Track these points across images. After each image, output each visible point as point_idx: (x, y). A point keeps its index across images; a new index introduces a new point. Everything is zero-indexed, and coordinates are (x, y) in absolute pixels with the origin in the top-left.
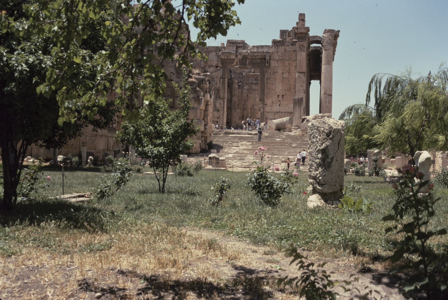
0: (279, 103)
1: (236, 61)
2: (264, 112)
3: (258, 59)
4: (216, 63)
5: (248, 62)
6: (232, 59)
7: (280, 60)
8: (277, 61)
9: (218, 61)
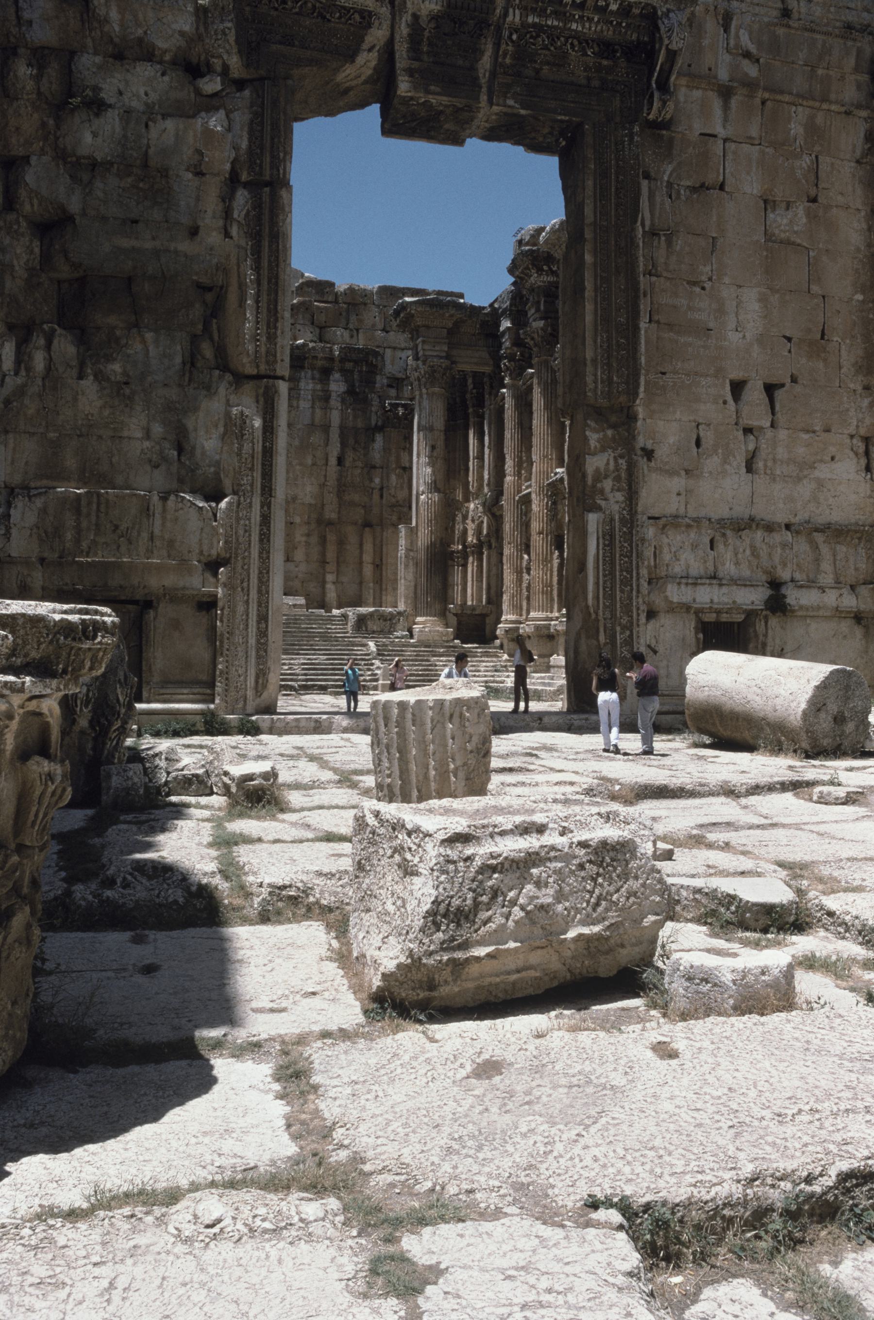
0: (742, 447)
1: (377, 35)
2: (630, 520)
3: (583, 41)
7: (751, 85)
8: (726, 93)
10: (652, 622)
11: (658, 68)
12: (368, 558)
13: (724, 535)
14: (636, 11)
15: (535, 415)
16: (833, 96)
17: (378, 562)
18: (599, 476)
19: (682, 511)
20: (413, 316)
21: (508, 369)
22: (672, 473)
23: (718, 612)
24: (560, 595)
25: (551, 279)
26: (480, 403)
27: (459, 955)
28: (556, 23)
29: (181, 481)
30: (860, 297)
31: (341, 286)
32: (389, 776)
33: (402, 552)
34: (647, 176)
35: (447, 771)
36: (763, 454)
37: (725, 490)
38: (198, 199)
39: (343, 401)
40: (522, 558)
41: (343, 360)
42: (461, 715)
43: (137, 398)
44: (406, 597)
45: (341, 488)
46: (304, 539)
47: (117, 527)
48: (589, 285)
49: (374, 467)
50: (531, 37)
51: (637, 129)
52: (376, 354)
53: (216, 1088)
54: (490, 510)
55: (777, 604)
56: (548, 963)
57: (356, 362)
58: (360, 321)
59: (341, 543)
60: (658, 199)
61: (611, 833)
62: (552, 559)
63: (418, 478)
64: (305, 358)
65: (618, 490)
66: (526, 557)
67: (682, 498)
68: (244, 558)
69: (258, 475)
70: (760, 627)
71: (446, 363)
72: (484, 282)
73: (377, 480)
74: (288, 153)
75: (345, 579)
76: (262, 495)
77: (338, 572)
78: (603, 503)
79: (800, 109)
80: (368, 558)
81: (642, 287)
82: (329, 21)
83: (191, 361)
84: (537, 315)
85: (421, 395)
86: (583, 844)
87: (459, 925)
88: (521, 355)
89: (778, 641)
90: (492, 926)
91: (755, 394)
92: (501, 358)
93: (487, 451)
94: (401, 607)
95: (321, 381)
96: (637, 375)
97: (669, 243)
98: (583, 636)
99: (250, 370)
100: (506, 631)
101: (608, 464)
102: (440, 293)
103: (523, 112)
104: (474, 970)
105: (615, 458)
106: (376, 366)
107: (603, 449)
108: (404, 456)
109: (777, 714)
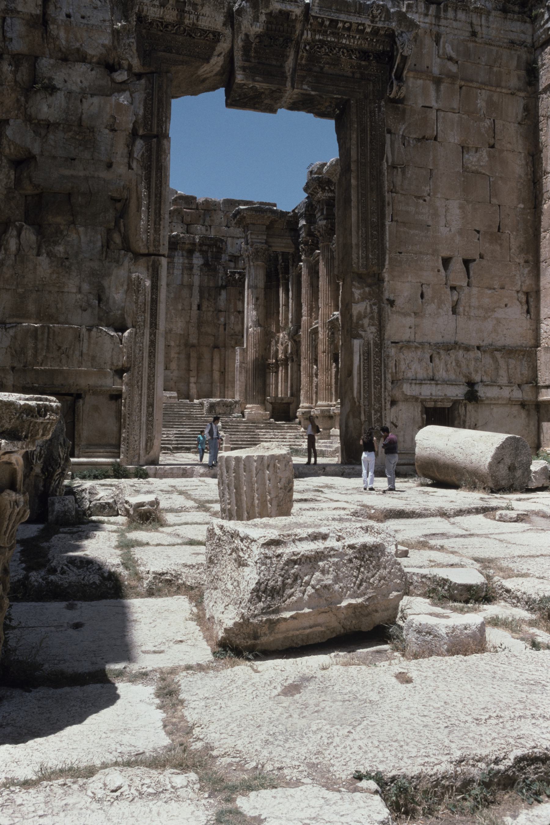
0: (449, 298)
1: (223, 46)
2: (380, 344)
3: (350, 50)
4: (106, 40)
5: (290, 63)
6: (204, 32)
7: (453, 77)
8: (438, 82)
9: (116, 33)
10: (395, 407)
11: (396, 67)
12: (216, 367)
13: (439, 353)
14: (382, 32)
15: (321, 279)
16: (503, 84)
17: (222, 370)
18: (360, 317)
19: (412, 338)
20: (245, 217)
21: (303, 250)
22: (406, 315)
23: (435, 401)
24: (336, 391)
25: (330, 195)
26: (286, 271)
27: (273, 617)
28: (333, 39)
29: (100, 319)
30: (521, 206)
31: (200, 199)
32: (229, 504)
33: (237, 364)
34: (389, 132)
35: (266, 501)
36: (463, 302)
37: (439, 325)
38: (112, 146)
39: (201, 270)
40: (312, 368)
41: (201, 245)
42: (275, 465)
43: (73, 268)
44: (240, 392)
45: (200, 323)
46: (176, 355)
47: (60, 348)
48: (354, 198)
49: (221, 311)
50: (318, 48)
51: (383, 103)
52: (222, 241)
53: (119, 702)
54: (292, 338)
55: (472, 396)
56: (330, 622)
57: (210, 246)
58: (212, 220)
59: (200, 358)
60: (396, 145)
61: (369, 539)
62: (331, 368)
63: (248, 318)
64: (178, 243)
65: (373, 325)
66: (315, 367)
67: (412, 330)
68: (139, 367)
69: (148, 315)
70: (462, 411)
71: (265, 246)
72: (289, 197)
73: (222, 319)
74: (168, 118)
75: (201, 381)
76: (151, 328)
77: (198, 377)
78: (363, 333)
79: (483, 91)
80: (216, 367)
81: (387, 199)
82: (194, 38)
83: (107, 244)
84: (322, 217)
85: (250, 266)
86: (351, 547)
87: (273, 598)
88: (312, 242)
89: (473, 419)
90: (294, 598)
91: (457, 266)
92: (300, 243)
93: (290, 301)
94: (237, 398)
95: (187, 257)
96: (384, 254)
97: (403, 173)
98: (351, 417)
99: (144, 251)
100: (303, 413)
101: (366, 309)
102: (261, 203)
103: (313, 93)
104: (282, 626)
105: (371, 305)
106: (222, 248)
107: (363, 299)
108: (239, 304)
109: (473, 465)
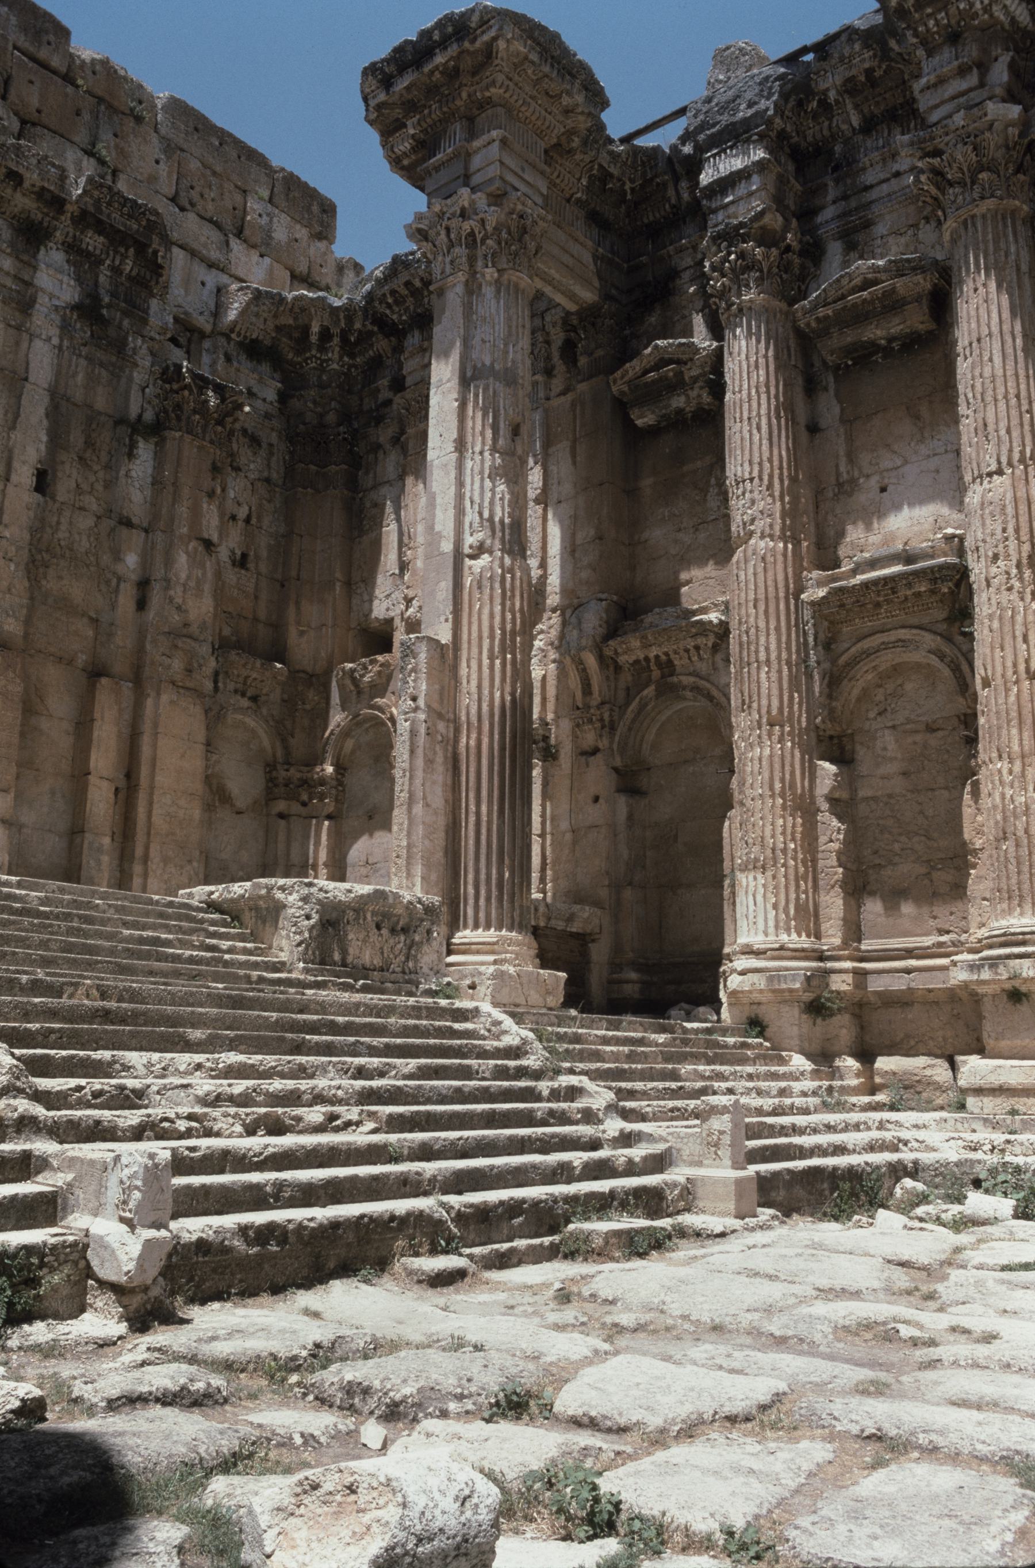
12: (104, 760)
39: (65, 328)
41: (85, 219)
49: (128, 523)
57: (117, 238)
58: (122, 153)
73: (131, 560)
80: (104, 760)
85: (472, 288)
